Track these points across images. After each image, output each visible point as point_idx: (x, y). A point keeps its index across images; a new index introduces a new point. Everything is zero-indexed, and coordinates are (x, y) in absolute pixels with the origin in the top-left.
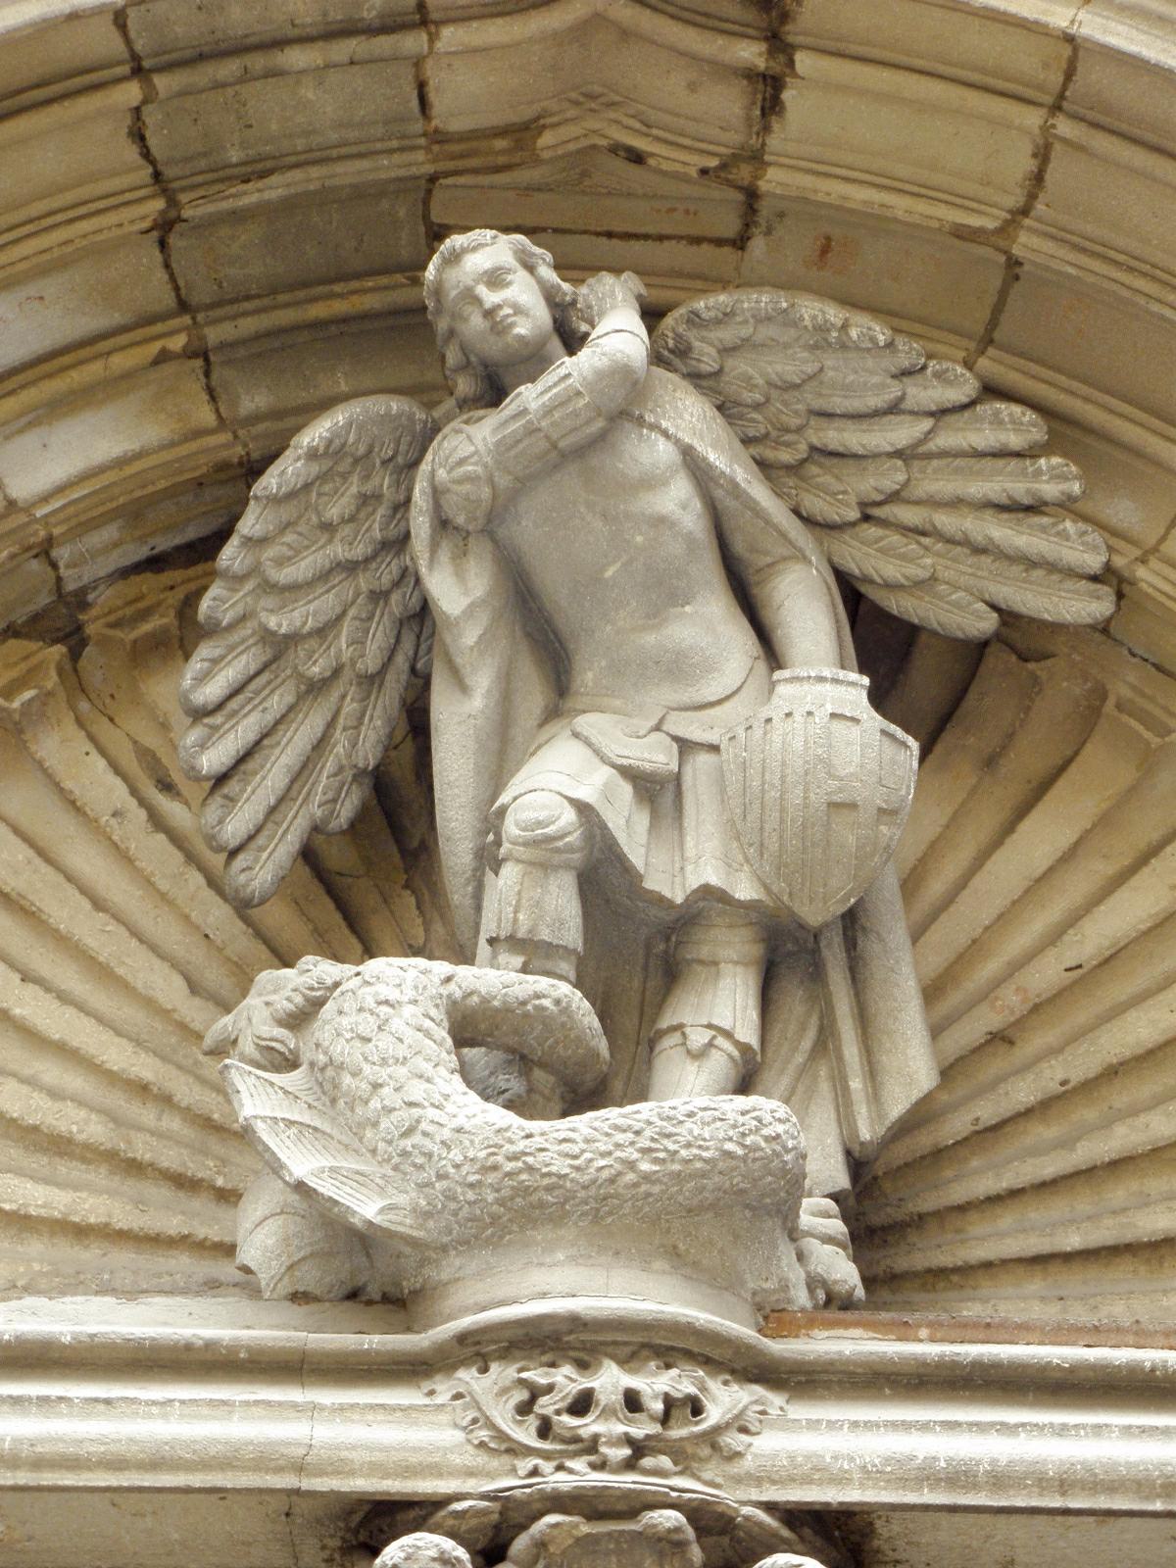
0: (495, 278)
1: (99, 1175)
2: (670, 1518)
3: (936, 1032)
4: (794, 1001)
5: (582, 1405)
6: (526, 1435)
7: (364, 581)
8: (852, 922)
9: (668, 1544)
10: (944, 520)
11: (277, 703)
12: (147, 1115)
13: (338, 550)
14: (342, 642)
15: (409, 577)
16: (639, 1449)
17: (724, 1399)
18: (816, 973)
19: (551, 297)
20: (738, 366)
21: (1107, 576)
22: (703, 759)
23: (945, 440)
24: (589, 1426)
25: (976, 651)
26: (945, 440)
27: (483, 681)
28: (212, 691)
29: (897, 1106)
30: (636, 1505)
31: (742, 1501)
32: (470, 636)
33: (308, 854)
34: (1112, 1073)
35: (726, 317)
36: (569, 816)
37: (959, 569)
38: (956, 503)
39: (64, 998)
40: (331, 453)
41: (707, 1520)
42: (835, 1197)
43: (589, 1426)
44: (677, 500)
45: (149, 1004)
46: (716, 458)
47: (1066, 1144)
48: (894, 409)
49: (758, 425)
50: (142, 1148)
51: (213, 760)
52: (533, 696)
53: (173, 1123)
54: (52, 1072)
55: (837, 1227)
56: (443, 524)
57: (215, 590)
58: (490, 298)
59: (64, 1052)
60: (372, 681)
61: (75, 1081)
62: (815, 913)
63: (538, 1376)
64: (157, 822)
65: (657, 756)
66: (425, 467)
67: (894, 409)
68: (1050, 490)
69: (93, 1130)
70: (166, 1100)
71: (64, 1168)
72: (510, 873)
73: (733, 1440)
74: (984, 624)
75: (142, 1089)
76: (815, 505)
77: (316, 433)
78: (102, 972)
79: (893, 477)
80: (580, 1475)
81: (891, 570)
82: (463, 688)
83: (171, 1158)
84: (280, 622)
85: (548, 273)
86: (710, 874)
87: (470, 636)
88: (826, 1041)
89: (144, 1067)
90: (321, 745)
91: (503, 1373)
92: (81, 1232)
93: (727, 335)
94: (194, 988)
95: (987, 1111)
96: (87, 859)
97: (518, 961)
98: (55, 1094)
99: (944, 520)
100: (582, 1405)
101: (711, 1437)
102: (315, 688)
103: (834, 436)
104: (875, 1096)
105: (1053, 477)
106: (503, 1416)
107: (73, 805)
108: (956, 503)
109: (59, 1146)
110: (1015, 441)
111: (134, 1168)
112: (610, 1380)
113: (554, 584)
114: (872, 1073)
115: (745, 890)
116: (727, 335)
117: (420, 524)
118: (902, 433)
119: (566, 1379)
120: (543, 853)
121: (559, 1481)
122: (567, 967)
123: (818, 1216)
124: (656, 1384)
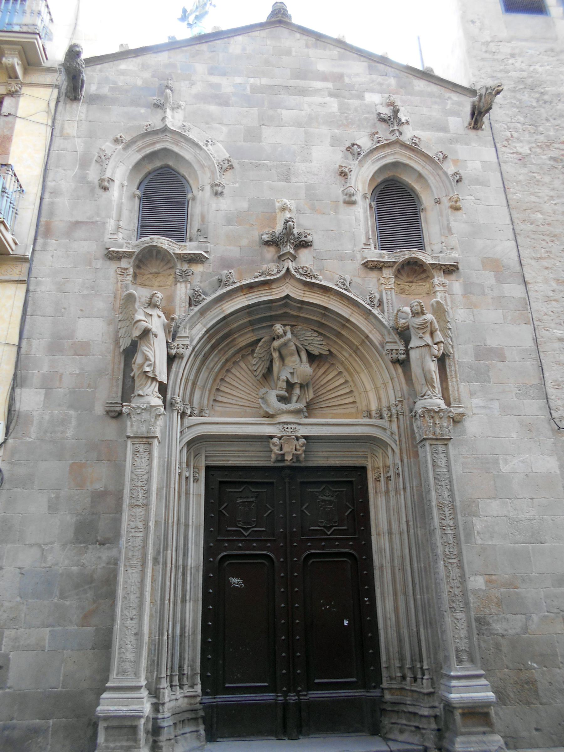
0: (278, 329)
2: (294, 437)
3: (313, 388)
5: (287, 428)
6: (283, 430)
7: (267, 352)
8: (307, 385)
9: (294, 439)
10: (315, 345)
11: (260, 363)
13: (265, 350)
14: (265, 357)
15: (270, 351)
16: (292, 432)
17: (298, 427)
18: (304, 387)
19: (283, 330)
22: (295, 370)
23: (315, 339)
24: (288, 430)
25: (317, 356)
28: (255, 363)
29: (311, 398)
30: (291, 436)
31: (299, 435)
32: (277, 359)
33: (263, 375)
37: (315, 349)
38: (316, 344)
40: (265, 342)
41: (295, 436)
42: (305, 407)
43: (288, 430)
44: (294, 348)
47: (324, 397)
48: (311, 336)
52: (281, 363)
55: (306, 410)
56: (274, 349)
58: (278, 331)
59: (243, 391)
60: (267, 360)
62: (304, 384)
63: (284, 426)
65: (292, 371)
67: (311, 336)
68: (324, 343)
72: (280, 382)
73: (298, 431)
76: (304, 343)
77: (263, 340)
80: (288, 434)
81: (310, 349)
82: (276, 363)
85: (283, 328)
86: (296, 381)
90: (264, 366)
91: (281, 426)
95: (317, 395)
97: (281, 389)
99: (315, 345)
100: (287, 428)
101: (297, 431)
103: (306, 338)
104: (309, 398)
106: (282, 429)
108: (316, 344)
110: (321, 339)
112: (289, 426)
114: (308, 396)
115: (299, 382)
118: (312, 338)
119: (286, 426)
120: (283, 381)
121: (285, 434)
122: (285, 389)
123: (305, 410)
124: (293, 427)
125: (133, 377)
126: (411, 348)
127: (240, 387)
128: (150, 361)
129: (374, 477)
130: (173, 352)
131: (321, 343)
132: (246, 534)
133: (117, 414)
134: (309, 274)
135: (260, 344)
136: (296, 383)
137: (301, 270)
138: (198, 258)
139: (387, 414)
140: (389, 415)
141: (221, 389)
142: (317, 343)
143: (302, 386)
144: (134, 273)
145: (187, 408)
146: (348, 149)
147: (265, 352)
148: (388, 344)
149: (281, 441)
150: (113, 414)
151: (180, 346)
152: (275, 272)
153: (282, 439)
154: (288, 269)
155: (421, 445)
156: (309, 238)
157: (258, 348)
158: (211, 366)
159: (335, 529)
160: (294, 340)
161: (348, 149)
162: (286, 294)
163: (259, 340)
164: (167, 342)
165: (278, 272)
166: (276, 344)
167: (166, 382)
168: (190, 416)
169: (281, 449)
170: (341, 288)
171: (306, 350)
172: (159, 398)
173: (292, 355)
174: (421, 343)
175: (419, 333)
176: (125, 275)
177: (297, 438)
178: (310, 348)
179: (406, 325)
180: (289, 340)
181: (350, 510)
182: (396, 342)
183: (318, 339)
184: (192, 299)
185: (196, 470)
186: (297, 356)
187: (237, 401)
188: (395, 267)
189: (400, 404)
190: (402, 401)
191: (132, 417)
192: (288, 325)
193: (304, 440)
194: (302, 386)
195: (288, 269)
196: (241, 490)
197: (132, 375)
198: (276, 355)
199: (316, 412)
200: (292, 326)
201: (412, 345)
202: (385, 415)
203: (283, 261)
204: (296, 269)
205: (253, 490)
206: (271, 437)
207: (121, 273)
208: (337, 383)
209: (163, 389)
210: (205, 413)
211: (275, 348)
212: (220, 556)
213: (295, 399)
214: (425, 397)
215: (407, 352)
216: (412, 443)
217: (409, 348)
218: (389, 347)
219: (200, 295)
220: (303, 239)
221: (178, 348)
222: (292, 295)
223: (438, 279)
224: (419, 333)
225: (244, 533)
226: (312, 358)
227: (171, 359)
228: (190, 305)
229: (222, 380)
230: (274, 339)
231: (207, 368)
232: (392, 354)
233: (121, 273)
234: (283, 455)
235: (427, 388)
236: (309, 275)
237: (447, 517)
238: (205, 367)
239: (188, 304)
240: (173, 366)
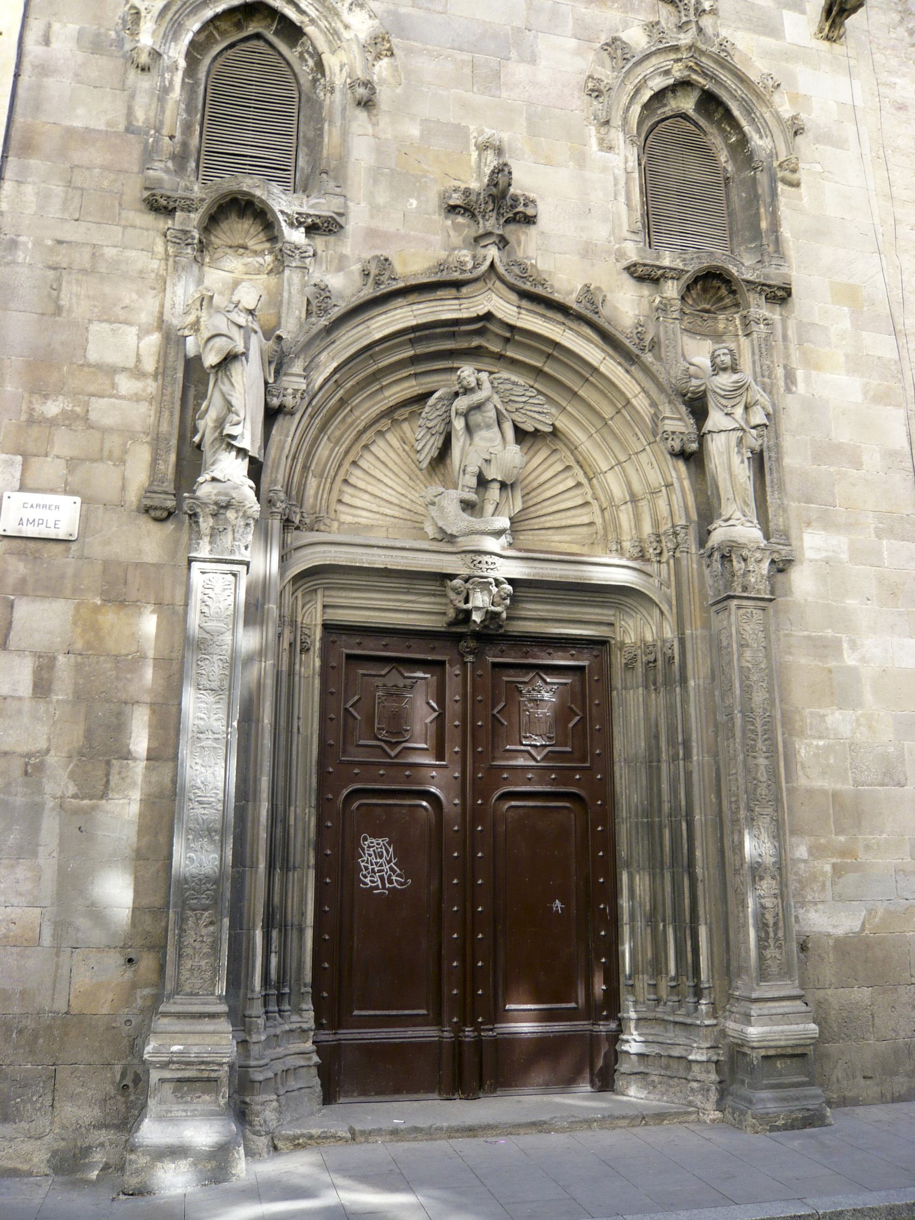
0: (469, 376)
1: (397, 508)
4: (504, 495)
5: (480, 562)
6: (472, 566)
10: (528, 413)
11: (428, 437)
12: (403, 498)
13: (438, 413)
20: (501, 386)
21: (553, 425)
23: (531, 401)
24: (480, 566)
26: (531, 401)
27: (462, 440)
28: (419, 437)
34: (544, 500)
35: (500, 378)
36: (477, 468)
37: (529, 421)
39: (391, 479)
40: (440, 399)
44: (492, 414)
45: (404, 481)
46: (499, 406)
49: (502, 395)
50: (403, 505)
51: (419, 448)
52: (468, 442)
53: (407, 500)
54: (389, 490)
56: (457, 413)
57: (421, 420)
61: (392, 492)
62: (509, 482)
64: (404, 450)
65: (488, 457)
66: (454, 404)
69: (396, 502)
70: (406, 497)
71: (392, 506)
74: (532, 429)
75: (403, 495)
76: (509, 408)
77: (436, 395)
78: (396, 475)
79: (521, 405)
81: (519, 420)
82: (458, 440)
83: (408, 507)
84: (429, 426)
87: (461, 433)
88: (507, 498)
89: (403, 492)
92: (395, 517)
93: (499, 381)
94: (410, 478)
96: (393, 455)
98: (390, 495)
99: (528, 413)
100: (480, 562)
102: (433, 435)
103: (513, 398)
105: (547, 408)
107: (391, 446)
109: (391, 503)
111: (402, 507)
113: (471, 423)
116: (499, 381)
117: (453, 414)
118: (524, 399)
125: (199, 446)
126: (710, 432)
127: (386, 480)
128: (238, 415)
129: (624, 661)
130: (275, 402)
131: (541, 410)
132: (393, 754)
133: (165, 514)
134: (531, 276)
135: (432, 400)
136: (494, 480)
137: (516, 270)
138: (326, 225)
139: (655, 549)
140: (658, 551)
141: (350, 481)
142: (534, 409)
143: (503, 485)
144: (200, 242)
145: (295, 512)
146: (606, 47)
147: (439, 419)
148: (667, 421)
149: (468, 585)
150: (158, 514)
151: (290, 391)
152: (470, 266)
153: (471, 581)
154: (492, 265)
155: (714, 608)
156: (530, 211)
157: (427, 409)
158: (338, 433)
159: (550, 752)
160: (496, 399)
161: (606, 47)
162: (485, 310)
163: (430, 394)
164: (266, 383)
165: (474, 267)
166: (462, 403)
167: (261, 459)
168: (297, 528)
169: (467, 601)
170: (587, 309)
171: (513, 421)
172: (251, 488)
173: (488, 426)
174: (728, 423)
175: (726, 407)
176: (183, 245)
177: (498, 583)
178: (518, 418)
179: (702, 388)
180: (488, 399)
181: (577, 718)
182: (680, 419)
183: (536, 402)
184: (314, 302)
185: (307, 632)
186: (496, 429)
187: (378, 506)
188: (682, 281)
189: (684, 531)
190: (685, 527)
191: (201, 520)
192: (485, 371)
193: (510, 588)
194: (503, 485)
195: (492, 265)
196: (383, 673)
197: (197, 439)
198: (459, 424)
199: (521, 537)
200: (491, 373)
201: (709, 425)
202: (651, 550)
203: (485, 246)
204: (508, 266)
205: (406, 674)
206: (452, 577)
207: (174, 240)
208: (561, 488)
209: (256, 470)
210: (325, 524)
211: (460, 411)
212: (345, 792)
213: (489, 508)
214: (730, 522)
215: (701, 438)
216: (701, 604)
217: (703, 431)
218: (670, 425)
219: (329, 297)
220: (520, 208)
221: (284, 396)
222: (499, 314)
223: (759, 308)
224: (726, 407)
225: (388, 750)
226: (521, 435)
227: (272, 415)
228: (309, 313)
229: (354, 463)
230: (457, 394)
231: (329, 439)
232: (673, 439)
233: (174, 240)
234: (468, 613)
235: (735, 506)
236: (531, 279)
237: (760, 737)
238: (326, 437)
239: (304, 315)
240: (274, 432)
